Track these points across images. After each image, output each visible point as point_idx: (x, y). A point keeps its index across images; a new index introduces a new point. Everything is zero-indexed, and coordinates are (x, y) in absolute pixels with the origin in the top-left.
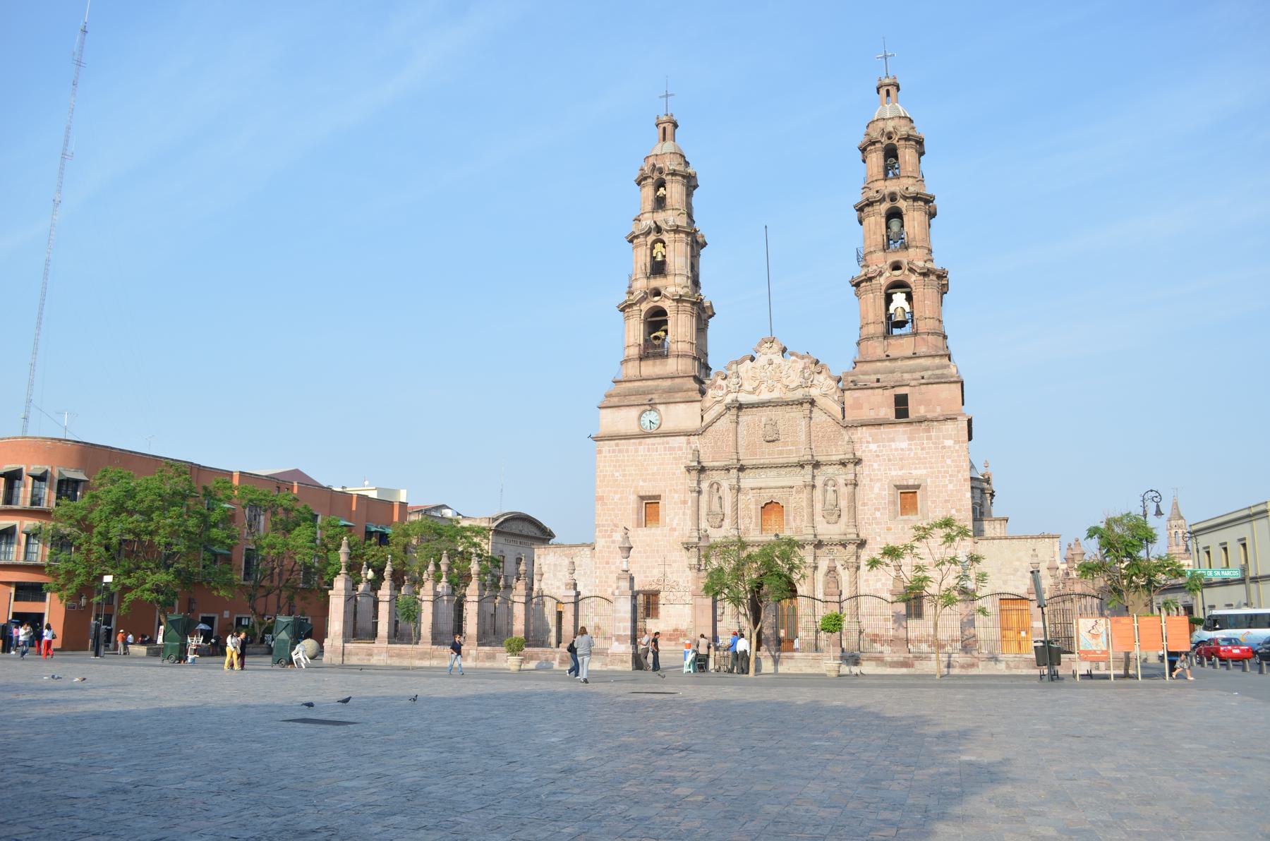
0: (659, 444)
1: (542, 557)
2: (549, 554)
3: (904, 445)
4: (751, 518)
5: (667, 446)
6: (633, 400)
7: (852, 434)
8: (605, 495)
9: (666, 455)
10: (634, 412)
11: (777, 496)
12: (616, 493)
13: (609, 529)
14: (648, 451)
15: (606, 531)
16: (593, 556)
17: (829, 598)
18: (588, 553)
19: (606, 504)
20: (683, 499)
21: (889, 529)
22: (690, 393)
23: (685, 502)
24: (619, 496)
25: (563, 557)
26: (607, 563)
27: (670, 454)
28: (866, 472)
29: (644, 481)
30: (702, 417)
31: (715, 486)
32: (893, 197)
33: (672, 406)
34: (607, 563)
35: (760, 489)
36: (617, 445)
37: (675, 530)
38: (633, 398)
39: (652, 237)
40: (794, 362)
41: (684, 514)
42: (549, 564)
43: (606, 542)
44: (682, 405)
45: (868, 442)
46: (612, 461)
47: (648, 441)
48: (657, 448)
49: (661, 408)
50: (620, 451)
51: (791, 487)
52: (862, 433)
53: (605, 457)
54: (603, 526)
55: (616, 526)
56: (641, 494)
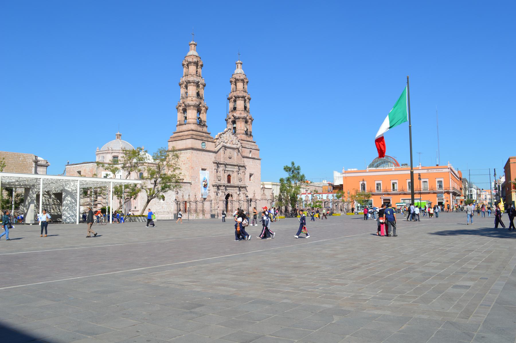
3: (252, 163)
6: (199, 138)
8: (194, 167)
10: (200, 142)
11: (231, 173)
12: (196, 167)
14: (204, 155)
15: (194, 178)
16: (190, 187)
17: (244, 201)
21: (249, 184)
22: (212, 139)
23: (212, 172)
24: (197, 168)
26: (194, 189)
29: (203, 164)
33: (208, 142)
34: (194, 189)
35: (228, 171)
38: (199, 137)
41: (212, 175)
43: (194, 182)
46: (195, 156)
50: (197, 154)
51: (233, 171)
55: (197, 177)
56: (203, 168)
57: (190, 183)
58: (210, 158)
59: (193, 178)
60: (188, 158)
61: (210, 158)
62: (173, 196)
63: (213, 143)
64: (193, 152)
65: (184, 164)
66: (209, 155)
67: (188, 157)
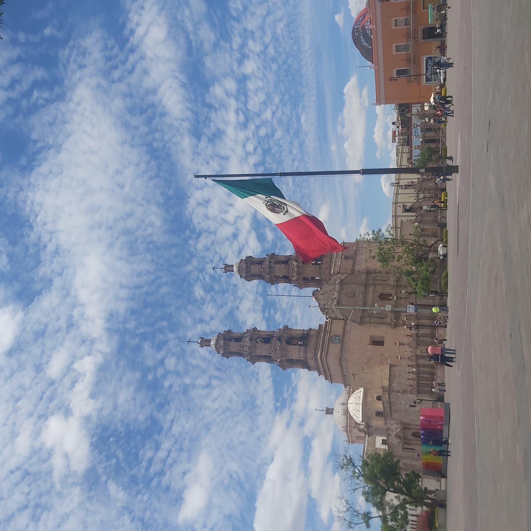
0: (347, 335)
1: (394, 389)
2: (393, 386)
4: (384, 304)
5: (349, 332)
7: (356, 271)
9: (352, 333)
13: (383, 357)
15: (384, 359)
16: (396, 366)
18: (393, 368)
19: (371, 359)
20: (373, 327)
24: (368, 353)
25: (395, 379)
27: (353, 330)
28: (372, 268)
30: (339, 319)
31: (370, 315)
32: (270, 262)
36: (345, 352)
37: (386, 332)
39: (254, 342)
40: (324, 287)
42: (398, 386)
44: (332, 326)
45: (360, 267)
47: (345, 339)
48: (349, 336)
49: (332, 334)
52: (356, 268)
53: (349, 357)
54: (381, 360)
55: (382, 355)
57: (390, 368)
58: (355, 329)
59: (384, 362)
60: (355, 365)
61: (355, 329)
62: (409, 397)
63: (333, 322)
64: (345, 358)
65: (363, 370)
66: (351, 330)
67: (353, 365)
